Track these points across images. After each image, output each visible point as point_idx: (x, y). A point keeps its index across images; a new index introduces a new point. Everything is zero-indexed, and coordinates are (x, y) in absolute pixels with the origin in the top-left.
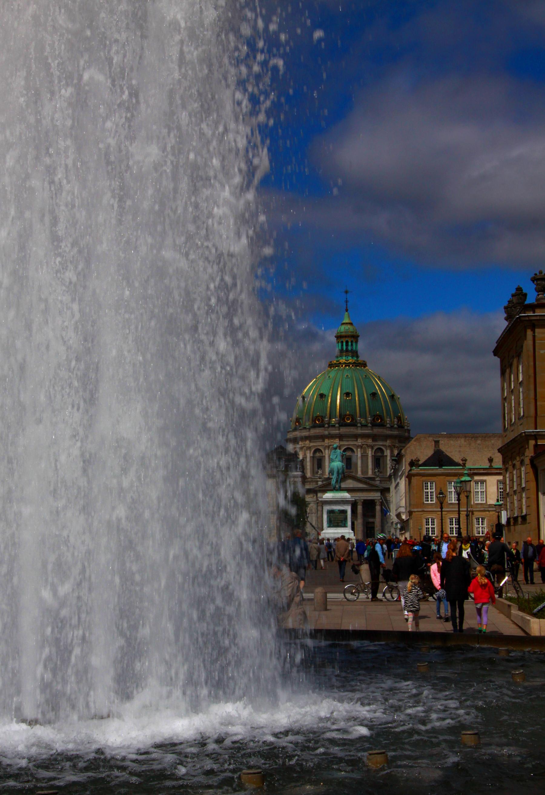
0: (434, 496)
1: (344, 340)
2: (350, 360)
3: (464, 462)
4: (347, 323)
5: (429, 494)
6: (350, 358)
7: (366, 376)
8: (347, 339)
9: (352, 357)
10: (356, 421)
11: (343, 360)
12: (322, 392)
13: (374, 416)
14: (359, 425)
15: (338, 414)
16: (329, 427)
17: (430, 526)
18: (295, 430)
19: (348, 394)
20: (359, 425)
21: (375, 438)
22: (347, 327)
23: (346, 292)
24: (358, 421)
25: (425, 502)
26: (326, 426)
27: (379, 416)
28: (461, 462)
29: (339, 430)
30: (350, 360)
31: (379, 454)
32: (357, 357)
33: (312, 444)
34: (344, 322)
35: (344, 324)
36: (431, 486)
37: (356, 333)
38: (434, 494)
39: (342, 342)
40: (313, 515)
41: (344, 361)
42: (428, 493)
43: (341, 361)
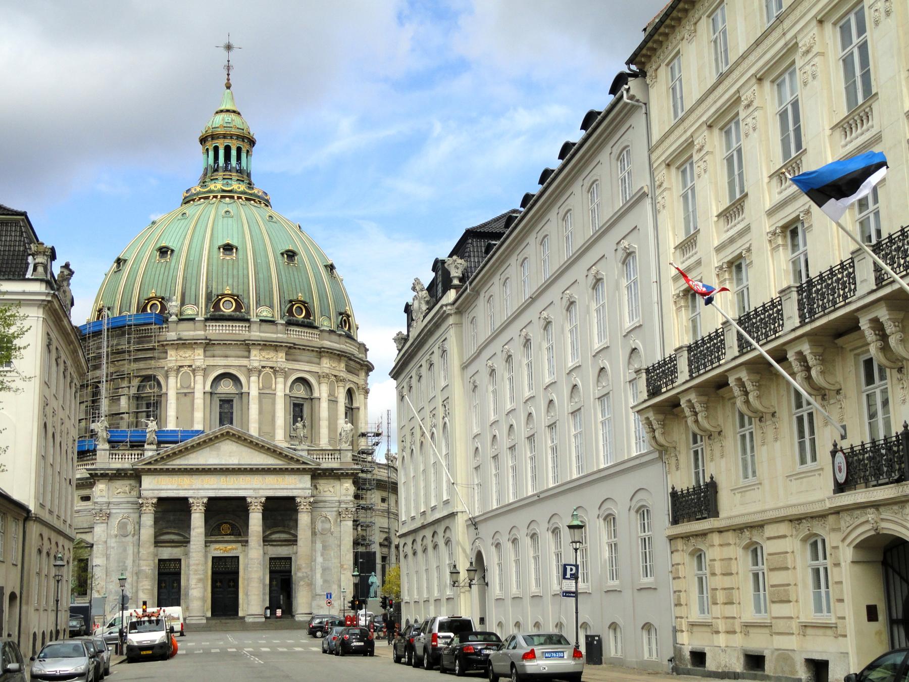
1: (221, 144)
2: (235, 186)
4: (228, 111)
8: (228, 142)
13: (291, 301)
16: (180, 320)
19: (228, 248)
21: (291, 350)
23: (229, 47)
27: (303, 303)
30: (235, 186)
31: (301, 392)
32: (250, 184)
34: (223, 107)
39: (216, 149)
40: (130, 539)
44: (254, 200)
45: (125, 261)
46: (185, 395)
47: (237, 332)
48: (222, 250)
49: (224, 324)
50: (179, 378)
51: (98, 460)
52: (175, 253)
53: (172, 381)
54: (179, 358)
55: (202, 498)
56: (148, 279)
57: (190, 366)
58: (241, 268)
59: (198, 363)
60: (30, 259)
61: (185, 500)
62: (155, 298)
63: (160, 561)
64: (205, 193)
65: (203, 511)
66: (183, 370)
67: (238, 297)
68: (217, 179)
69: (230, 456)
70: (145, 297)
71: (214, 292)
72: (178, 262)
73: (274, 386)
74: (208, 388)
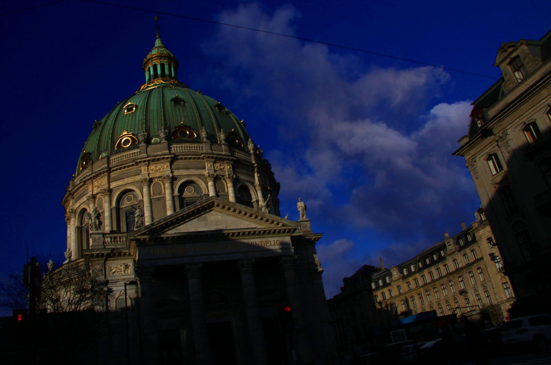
4: (160, 47)
39: (155, 67)
46: (158, 200)
47: (194, 151)
48: (173, 102)
49: (183, 146)
52: (139, 108)
57: (159, 177)
69: (217, 225)
71: (172, 126)
73: (226, 190)
74: (176, 193)
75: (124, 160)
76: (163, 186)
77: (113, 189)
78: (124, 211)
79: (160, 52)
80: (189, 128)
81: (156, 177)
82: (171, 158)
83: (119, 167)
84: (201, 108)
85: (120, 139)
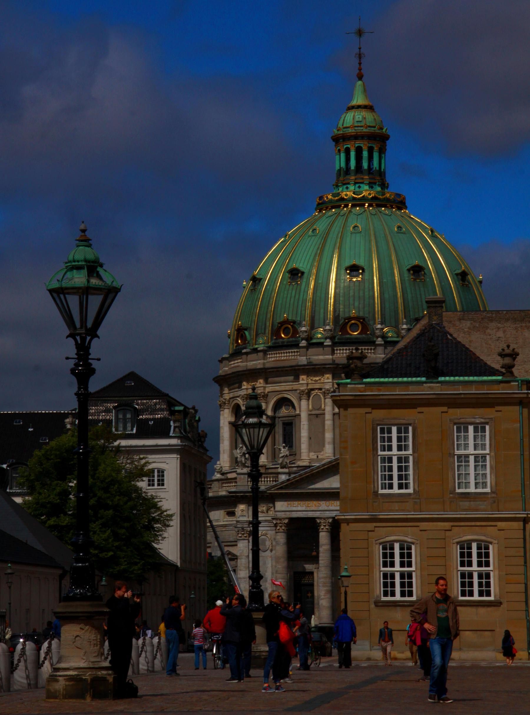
0: (411, 472)
2: (366, 191)
3: (508, 360)
4: (359, 107)
5: (395, 464)
6: (367, 187)
7: (399, 227)
9: (371, 185)
10: (373, 334)
11: (348, 193)
12: (294, 265)
14: (379, 341)
15: (330, 316)
16: (311, 345)
17: (397, 568)
18: (237, 354)
19: (354, 269)
20: (379, 341)
22: (359, 115)
23: (360, 33)
24: (378, 332)
25: (381, 491)
26: (303, 343)
28: (495, 363)
29: (333, 353)
30: (366, 191)
32: (384, 186)
33: (270, 388)
34: (354, 103)
35: (353, 107)
36: (399, 439)
37: (382, 129)
38: (411, 464)
39: (347, 151)
41: (350, 194)
42: (390, 460)
43: (343, 195)
44: (385, 206)
45: (260, 280)
50: (310, 400)
51: (239, 484)
52: (305, 275)
53: (304, 403)
54: (310, 382)
55: (328, 518)
56: (280, 302)
57: (320, 389)
58: (366, 290)
59: (328, 386)
60: (172, 423)
61: (313, 519)
62: (286, 322)
63: (295, 573)
64: (338, 200)
65: (329, 530)
66: (314, 393)
67: (364, 319)
68: (349, 184)
70: (278, 321)
71: (342, 315)
72: (308, 284)
75: (283, 358)
76: (323, 400)
77: (269, 394)
78: (281, 420)
79: (356, 124)
80: (361, 320)
81: (316, 389)
82: (334, 367)
83: (275, 370)
84: (385, 280)
85: (279, 325)
